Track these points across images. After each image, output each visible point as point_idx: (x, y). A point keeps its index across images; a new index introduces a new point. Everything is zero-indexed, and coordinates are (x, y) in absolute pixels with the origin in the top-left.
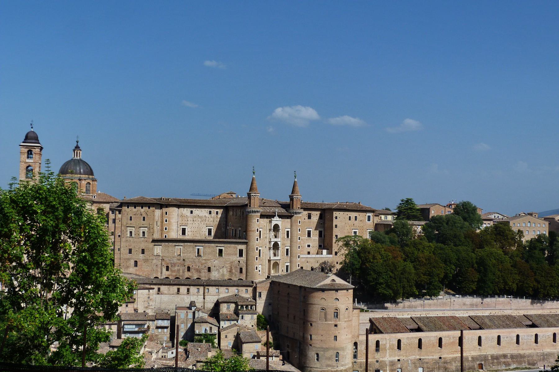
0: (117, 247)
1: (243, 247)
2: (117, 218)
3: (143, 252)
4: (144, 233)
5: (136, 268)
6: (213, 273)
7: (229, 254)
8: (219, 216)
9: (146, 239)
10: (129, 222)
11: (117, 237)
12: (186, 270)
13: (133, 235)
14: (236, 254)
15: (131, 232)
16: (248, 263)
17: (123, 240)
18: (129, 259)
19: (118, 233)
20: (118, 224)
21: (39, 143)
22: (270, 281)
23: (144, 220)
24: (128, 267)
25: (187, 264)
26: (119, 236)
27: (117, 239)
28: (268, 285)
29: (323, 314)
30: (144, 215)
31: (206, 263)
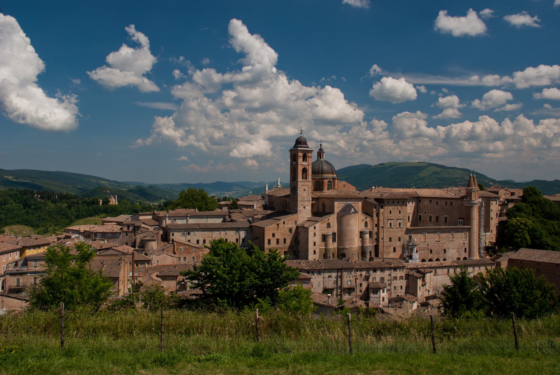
0: (381, 237)
4: (400, 223)
5: (394, 253)
7: (458, 238)
10: (390, 215)
13: (392, 226)
14: (462, 238)
15: (391, 224)
17: (385, 230)
18: (390, 246)
19: (381, 224)
20: (381, 218)
21: (308, 147)
23: (400, 213)
24: (389, 253)
25: (430, 247)
28: (507, 262)
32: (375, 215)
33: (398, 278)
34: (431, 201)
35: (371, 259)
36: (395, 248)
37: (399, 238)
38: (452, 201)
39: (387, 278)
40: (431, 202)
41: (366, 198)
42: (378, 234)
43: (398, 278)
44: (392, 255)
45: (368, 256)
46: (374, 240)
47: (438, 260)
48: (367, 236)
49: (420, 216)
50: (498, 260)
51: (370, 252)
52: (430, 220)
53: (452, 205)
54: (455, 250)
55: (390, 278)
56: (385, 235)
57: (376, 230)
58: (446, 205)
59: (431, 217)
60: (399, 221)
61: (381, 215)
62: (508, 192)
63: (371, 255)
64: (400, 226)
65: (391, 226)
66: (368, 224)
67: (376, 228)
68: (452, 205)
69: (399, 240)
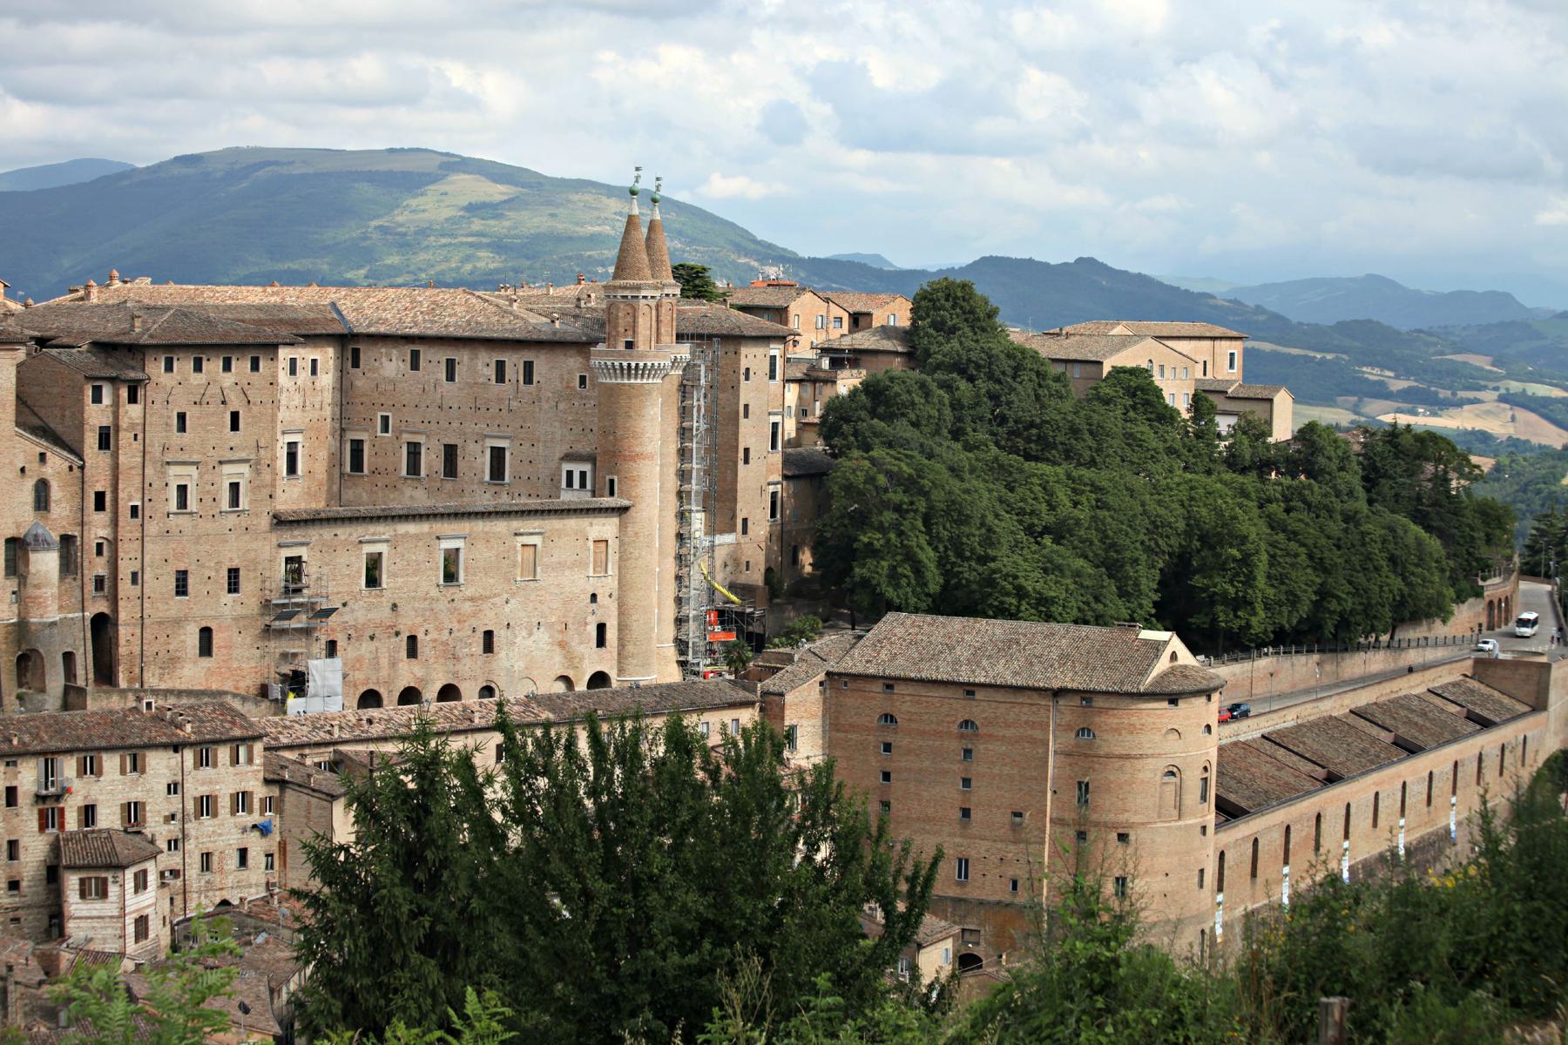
0: (126, 569)
1: (606, 527)
2: (124, 423)
3: (234, 583)
4: (235, 487)
5: (206, 662)
6: (502, 654)
7: (561, 565)
8: (327, 379)
9: (244, 521)
10: (176, 438)
11: (125, 512)
12: (404, 654)
14: (582, 565)
15: (182, 490)
16: (631, 602)
17: (152, 528)
18: (178, 622)
19: (129, 495)
20: (129, 454)
22: (821, 677)
23: (235, 426)
24: (173, 661)
25: (407, 625)
26: (134, 510)
27: (127, 524)
29: (1170, 791)
30: (236, 404)
31: (474, 615)
32: (91, 441)
33: (224, 804)
34: (415, 356)
35: (72, 696)
36: (206, 633)
37: (234, 574)
38: (528, 355)
39: (158, 806)
40: (415, 366)
41: (42, 342)
42: (110, 548)
43: (224, 804)
44: (194, 673)
45: (55, 682)
46: (90, 587)
47: (449, 692)
48: (46, 563)
49: (357, 447)
50: (771, 683)
51: (68, 657)
52: (414, 468)
53: (528, 379)
54: (543, 636)
55: (174, 804)
56: (151, 555)
57: (99, 527)
58: (500, 378)
59: (414, 451)
60: (230, 473)
61: (125, 438)
62: (836, 311)
63: (70, 673)
64: (235, 501)
65: (182, 503)
66: (56, 493)
67: (102, 518)
68: (528, 379)
69: (233, 587)
